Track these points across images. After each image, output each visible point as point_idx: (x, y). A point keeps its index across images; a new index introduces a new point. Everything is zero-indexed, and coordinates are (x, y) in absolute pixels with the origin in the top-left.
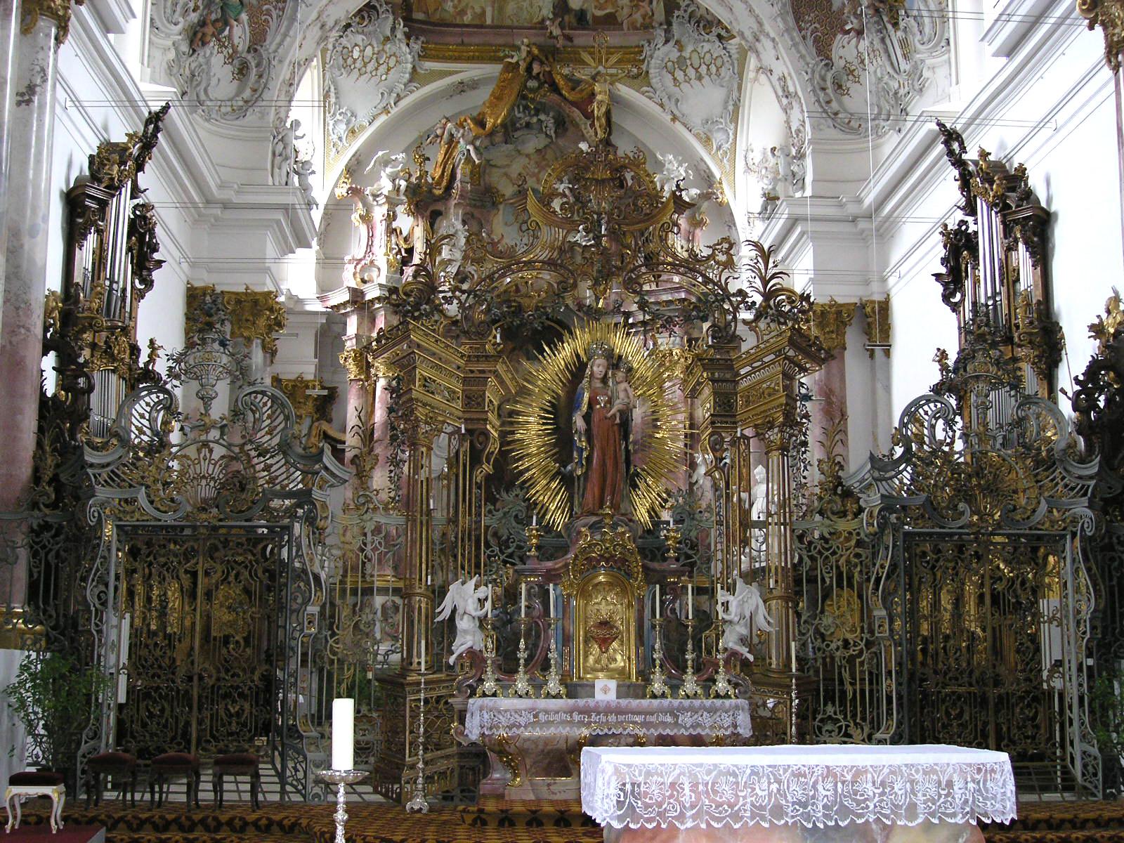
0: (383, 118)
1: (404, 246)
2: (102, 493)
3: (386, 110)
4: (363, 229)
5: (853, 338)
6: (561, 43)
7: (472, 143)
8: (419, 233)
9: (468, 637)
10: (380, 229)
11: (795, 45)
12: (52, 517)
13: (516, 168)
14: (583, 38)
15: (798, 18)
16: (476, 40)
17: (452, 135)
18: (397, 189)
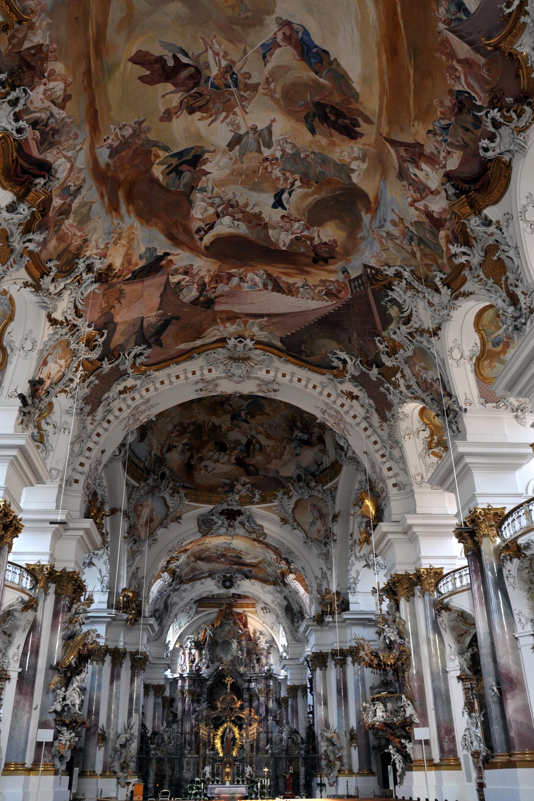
0: (188, 624)
2: (152, 752)
3: (189, 622)
4: (183, 656)
5: (300, 694)
7: (211, 630)
8: (197, 654)
9: (208, 776)
10: (187, 656)
12: (145, 756)
15: (286, 614)
16: (212, 602)
17: (206, 629)
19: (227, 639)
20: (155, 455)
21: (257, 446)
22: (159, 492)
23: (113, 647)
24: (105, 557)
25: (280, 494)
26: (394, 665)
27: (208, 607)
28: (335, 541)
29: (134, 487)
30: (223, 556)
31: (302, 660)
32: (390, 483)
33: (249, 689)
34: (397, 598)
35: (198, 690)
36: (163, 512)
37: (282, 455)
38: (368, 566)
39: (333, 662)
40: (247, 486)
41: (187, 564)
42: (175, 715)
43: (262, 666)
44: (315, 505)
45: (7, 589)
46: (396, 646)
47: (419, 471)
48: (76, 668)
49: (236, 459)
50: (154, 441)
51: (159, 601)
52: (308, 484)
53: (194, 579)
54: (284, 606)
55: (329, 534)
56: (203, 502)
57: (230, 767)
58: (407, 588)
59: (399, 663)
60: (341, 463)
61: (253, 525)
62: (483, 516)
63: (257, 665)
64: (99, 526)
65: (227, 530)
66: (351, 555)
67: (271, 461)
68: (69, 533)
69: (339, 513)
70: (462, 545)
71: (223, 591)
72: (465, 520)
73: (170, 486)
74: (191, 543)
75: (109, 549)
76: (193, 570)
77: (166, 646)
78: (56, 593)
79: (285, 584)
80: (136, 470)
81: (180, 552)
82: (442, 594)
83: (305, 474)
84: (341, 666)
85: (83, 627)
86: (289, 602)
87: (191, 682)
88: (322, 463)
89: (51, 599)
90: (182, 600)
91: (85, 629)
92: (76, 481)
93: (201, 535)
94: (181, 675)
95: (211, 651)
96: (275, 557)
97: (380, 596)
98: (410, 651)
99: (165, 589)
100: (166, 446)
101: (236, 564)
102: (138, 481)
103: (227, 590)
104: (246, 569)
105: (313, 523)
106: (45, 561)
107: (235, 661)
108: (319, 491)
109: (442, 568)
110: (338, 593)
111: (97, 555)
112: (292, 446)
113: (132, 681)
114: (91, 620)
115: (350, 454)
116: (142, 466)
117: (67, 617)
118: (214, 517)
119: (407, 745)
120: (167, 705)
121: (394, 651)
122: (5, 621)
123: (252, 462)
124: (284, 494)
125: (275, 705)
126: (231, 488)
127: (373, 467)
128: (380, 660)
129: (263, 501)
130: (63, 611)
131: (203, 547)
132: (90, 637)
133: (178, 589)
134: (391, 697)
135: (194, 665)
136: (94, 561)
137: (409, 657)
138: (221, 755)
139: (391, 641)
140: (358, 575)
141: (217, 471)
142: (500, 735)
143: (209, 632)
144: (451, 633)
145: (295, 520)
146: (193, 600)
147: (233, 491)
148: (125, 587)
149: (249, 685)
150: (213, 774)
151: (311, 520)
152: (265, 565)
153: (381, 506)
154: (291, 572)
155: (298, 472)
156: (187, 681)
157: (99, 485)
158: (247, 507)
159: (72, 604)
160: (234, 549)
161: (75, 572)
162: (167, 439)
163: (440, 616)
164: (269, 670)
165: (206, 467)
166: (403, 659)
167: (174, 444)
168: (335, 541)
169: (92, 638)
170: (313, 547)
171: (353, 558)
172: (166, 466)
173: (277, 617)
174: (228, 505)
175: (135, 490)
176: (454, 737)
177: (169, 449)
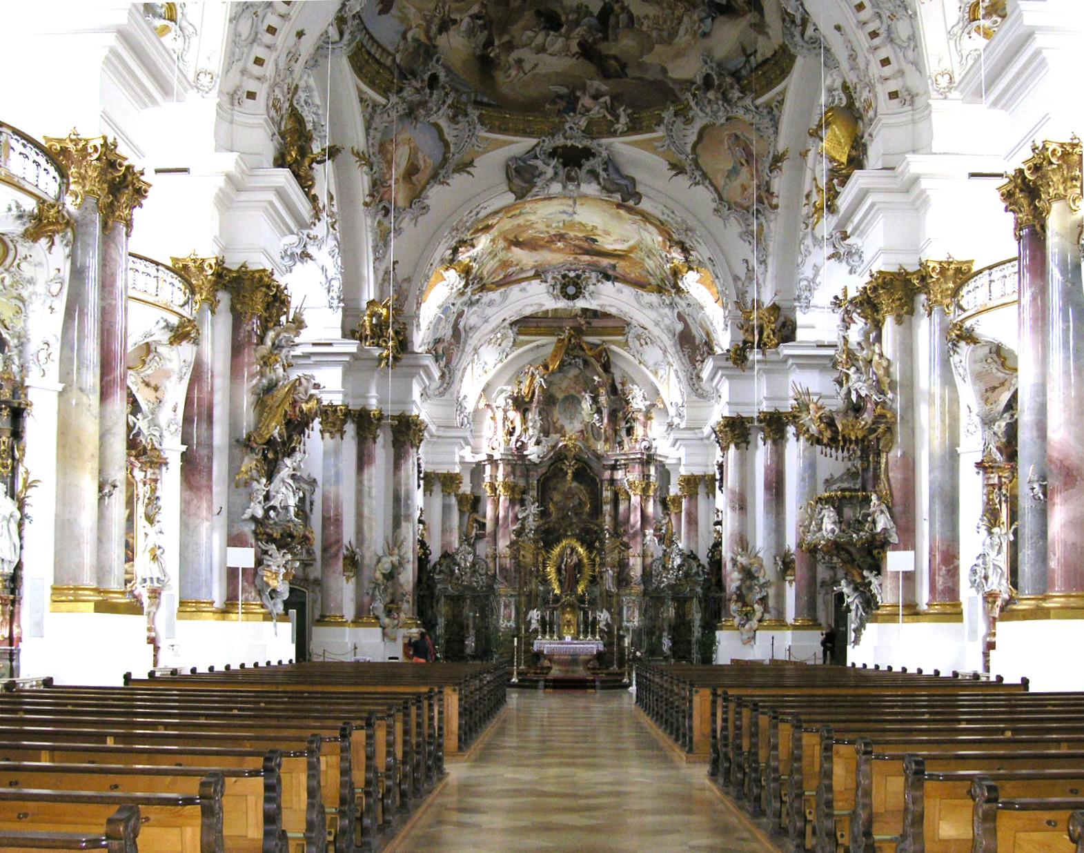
0: (500, 365)
1: (511, 426)
3: (501, 361)
5: (701, 490)
6: (584, 328)
7: (543, 377)
9: (534, 625)
11: (680, 359)
13: (564, 385)
14: (596, 323)
16: (543, 325)
17: (533, 374)
18: (507, 404)
19: (572, 392)
20: (416, 40)
21: (623, 18)
22: (428, 115)
23: (359, 408)
24: (332, 243)
25: (667, 115)
26: (863, 440)
27: (536, 335)
28: (776, 207)
29: (375, 105)
30: (561, 237)
31: (707, 430)
32: (882, 91)
33: (612, 481)
34: (880, 317)
35: (522, 483)
36: (438, 154)
37: (673, 34)
38: (835, 256)
39: (761, 435)
40: (602, 100)
41: (493, 254)
42: (483, 526)
43: (636, 440)
44: (737, 137)
45: (131, 303)
46: (869, 406)
47: (946, 65)
48: (284, 443)
49: (580, 45)
50: (412, 12)
51: (443, 323)
52: (724, 95)
53: (506, 282)
54: (677, 332)
55: (764, 195)
56: (517, 132)
57: (573, 612)
58: (900, 299)
59: (871, 437)
60: (792, 50)
61: (614, 176)
62: (1059, 159)
63: (626, 439)
64: (305, 181)
65: (564, 187)
66: (804, 238)
67: (652, 49)
68: (244, 196)
69: (783, 154)
70: (1011, 215)
71: (562, 304)
72: (1023, 167)
73: (449, 101)
74: (496, 213)
75: (336, 226)
76: (505, 264)
77: (460, 406)
78: (233, 309)
79: (679, 291)
80: (378, 72)
81: (477, 231)
82: (964, 311)
83: (720, 75)
84: (775, 442)
85: (289, 370)
86: (686, 326)
87: (509, 469)
88: (756, 51)
89: (224, 322)
90: (486, 321)
91: (294, 375)
92: (251, 95)
93: (513, 196)
94: (490, 457)
95: (545, 415)
96: (660, 239)
97: (847, 312)
98: (895, 416)
99: (452, 301)
100: (437, 21)
101: (587, 252)
102: (385, 92)
103: (571, 303)
104: (605, 262)
105: (733, 173)
106: (208, 252)
107: (589, 432)
108: (747, 110)
109: (971, 262)
110: (775, 308)
111: (315, 238)
112: (695, 17)
113: (397, 466)
114: (314, 359)
115: (810, 32)
116: (389, 62)
117: (258, 355)
118: (539, 163)
119: (873, 580)
120: (467, 508)
121: (865, 416)
122: (144, 362)
123: (613, 52)
124: (676, 115)
125: (660, 509)
126: (571, 104)
127: (853, 57)
128: (836, 432)
129: (634, 128)
130: (250, 343)
131: (521, 220)
132: (301, 389)
133: (478, 301)
134: (851, 497)
135: (514, 439)
136: (311, 250)
137: (890, 430)
138: (557, 591)
139: (859, 396)
140: (816, 275)
141: (542, 70)
142: (1033, 565)
143: (538, 379)
144: (974, 384)
145: (698, 167)
146: (506, 323)
147: (574, 110)
148: (372, 298)
149: (612, 474)
150: (543, 622)
151: (730, 167)
152: (641, 254)
153: (862, 137)
154: (690, 269)
155: (706, 70)
156: (501, 467)
157: (306, 102)
158: (604, 141)
159: (265, 329)
160: (580, 223)
161: (264, 270)
162: (437, 5)
163: (955, 352)
164: (649, 449)
165: (519, 62)
166: (880, 430)
167: (453, 16)
168: (776, 207)
169: (306, 392)
170: (732, 219)
171: (809, 241)
172: (438, 61)
173: (665, 352)
174: (566, 138)
175: (378, 111)
176: (957, 569)
177: (444, 26)
